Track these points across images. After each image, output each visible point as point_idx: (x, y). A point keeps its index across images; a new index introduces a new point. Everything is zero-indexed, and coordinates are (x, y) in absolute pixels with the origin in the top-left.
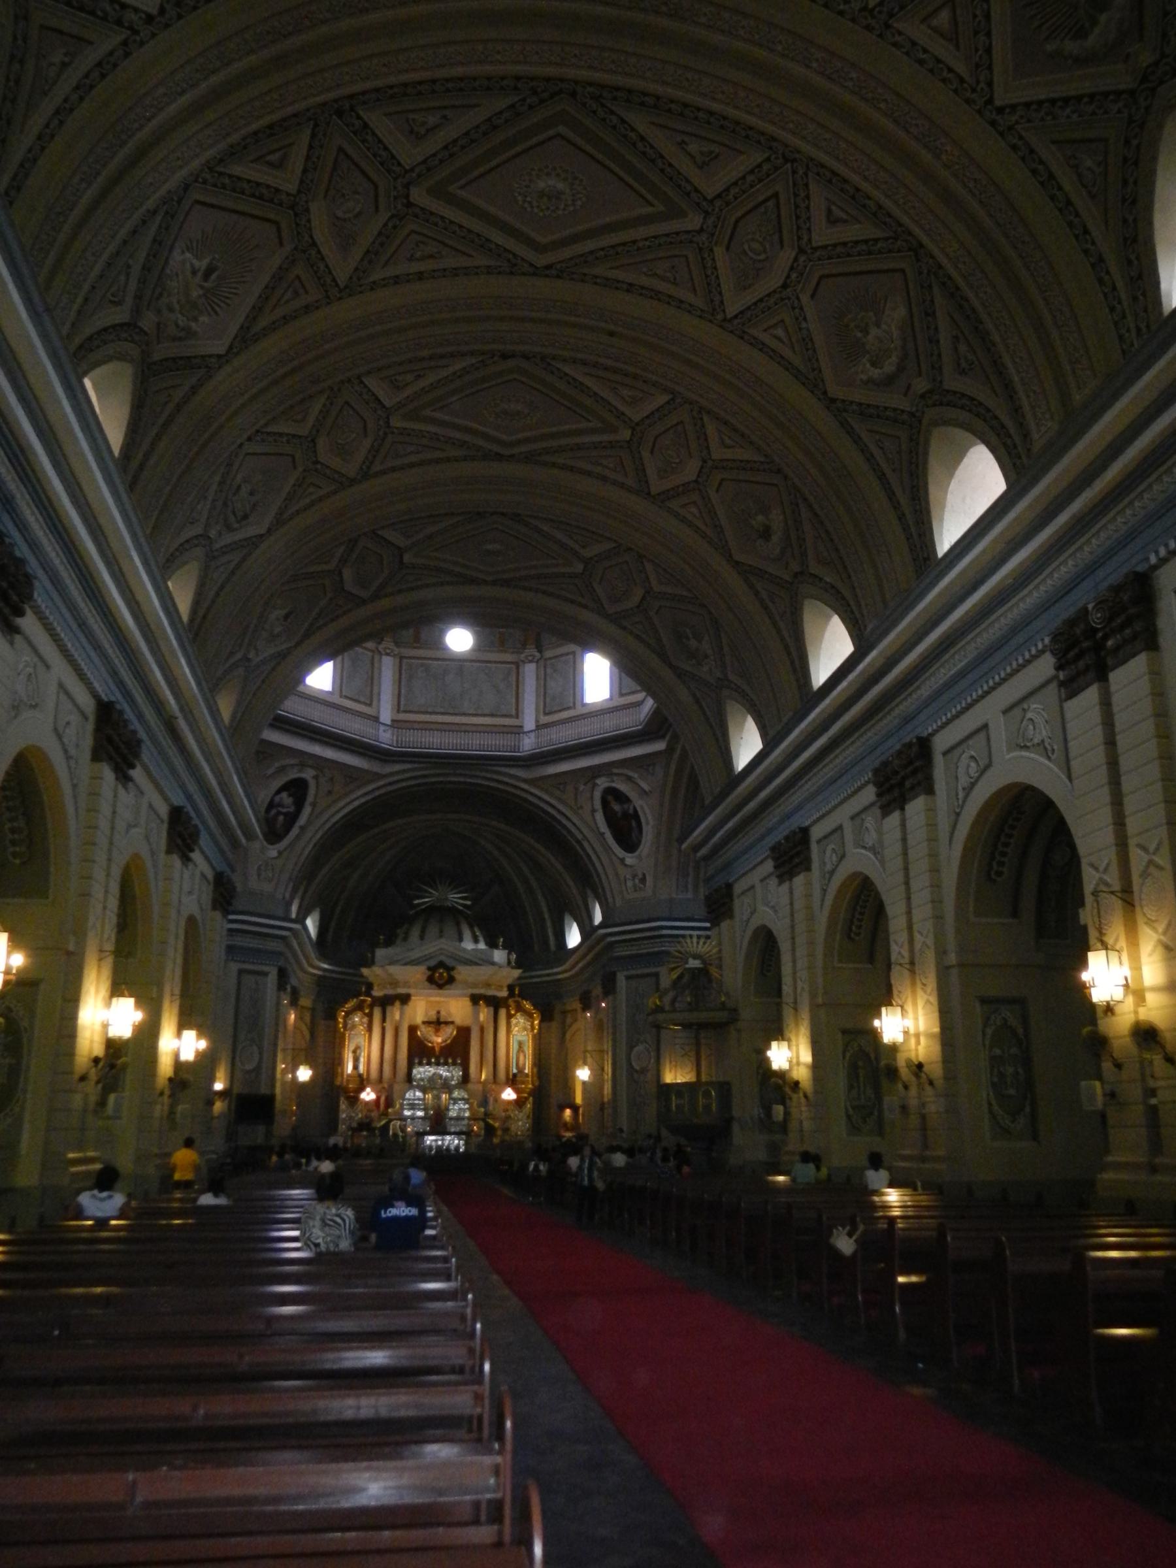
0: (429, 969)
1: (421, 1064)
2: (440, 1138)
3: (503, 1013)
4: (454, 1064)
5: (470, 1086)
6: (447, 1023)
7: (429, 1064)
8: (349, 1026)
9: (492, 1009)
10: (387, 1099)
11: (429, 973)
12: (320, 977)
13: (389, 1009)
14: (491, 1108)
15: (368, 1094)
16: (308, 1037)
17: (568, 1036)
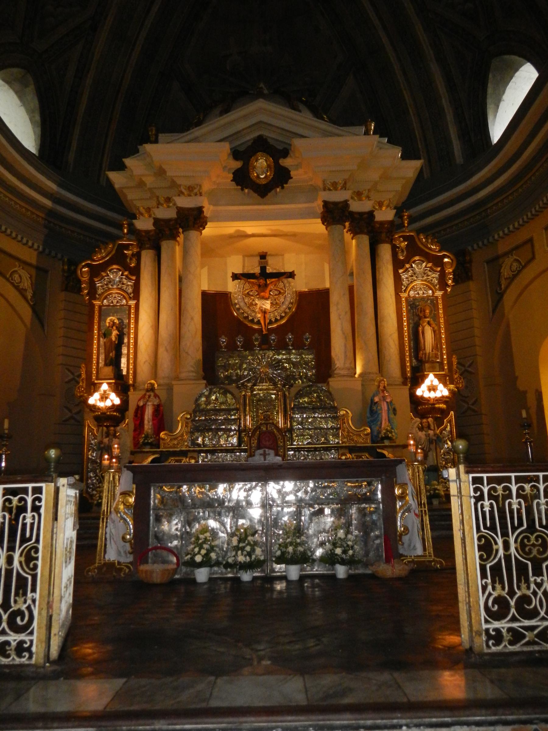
0: (236, 154)
1: (232, 347)
2: (256, 496)
3: (385, 251)
4: (299, 346)
5: (335, 383)
6: (278, 275)
7: (248, 346)
8: (100, 291)
9: (365, 239)
10: (157, 410)
11: (238, 165)
12: (51, 213)
13: (165, 245)
14: (385, 424)
15: (104, 397)
16: (26, 312)
17: (509, 298)
